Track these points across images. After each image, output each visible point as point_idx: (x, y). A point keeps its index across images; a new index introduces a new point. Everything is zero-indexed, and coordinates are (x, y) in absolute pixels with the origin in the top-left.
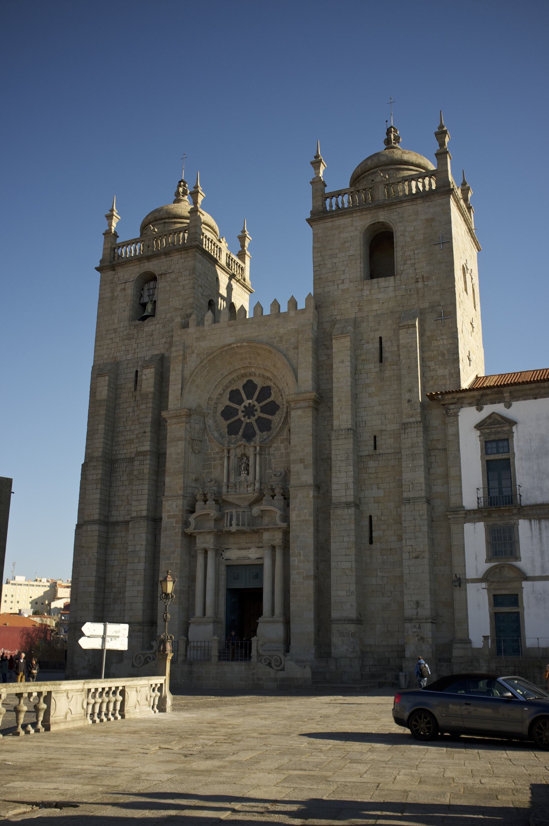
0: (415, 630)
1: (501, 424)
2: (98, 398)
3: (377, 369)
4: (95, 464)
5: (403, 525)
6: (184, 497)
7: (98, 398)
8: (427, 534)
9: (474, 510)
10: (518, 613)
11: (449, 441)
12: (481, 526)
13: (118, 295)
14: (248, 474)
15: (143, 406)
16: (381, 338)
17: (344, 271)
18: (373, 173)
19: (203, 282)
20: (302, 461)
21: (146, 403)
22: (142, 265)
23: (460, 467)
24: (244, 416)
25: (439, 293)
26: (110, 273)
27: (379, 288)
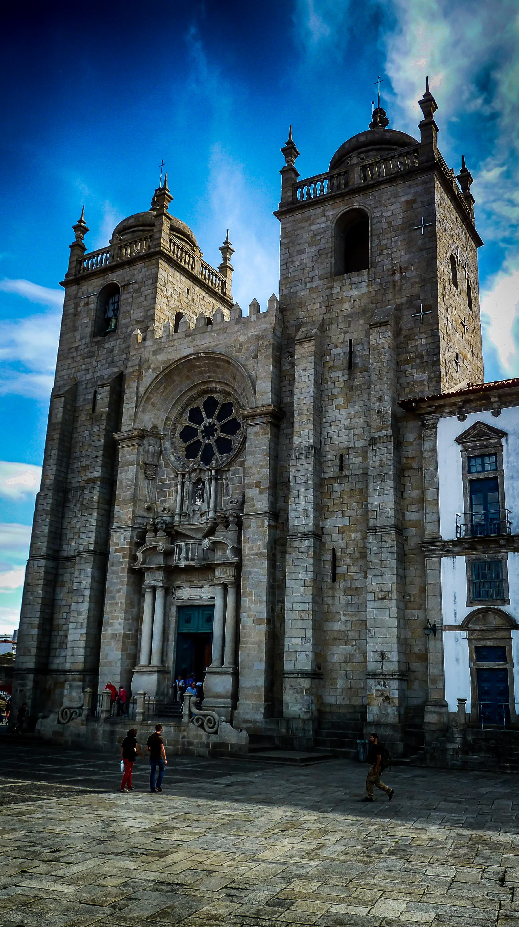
0: (379, 688)
1: (487, 436)
2: (54, 421)
3: (346, 377)
5: (369, 559)
6: (133, 528)
7: (54, 421)
8: (395, 570)
9: (453, 541)
10: (505, 670)
11: (425, 458)
12: (461, 561)
13: (81, 311)
14: (203, 501)
15: (96, 429)
17: (313, 267)
18: (350, 157)
19: (168, 292)
20: (257, 485)
21: (99, 425)
22: (106, 277)
23: (438, 489)
24: (203, 437)
25: (418, 285)
26: (74, 288)
27: (351, 284)
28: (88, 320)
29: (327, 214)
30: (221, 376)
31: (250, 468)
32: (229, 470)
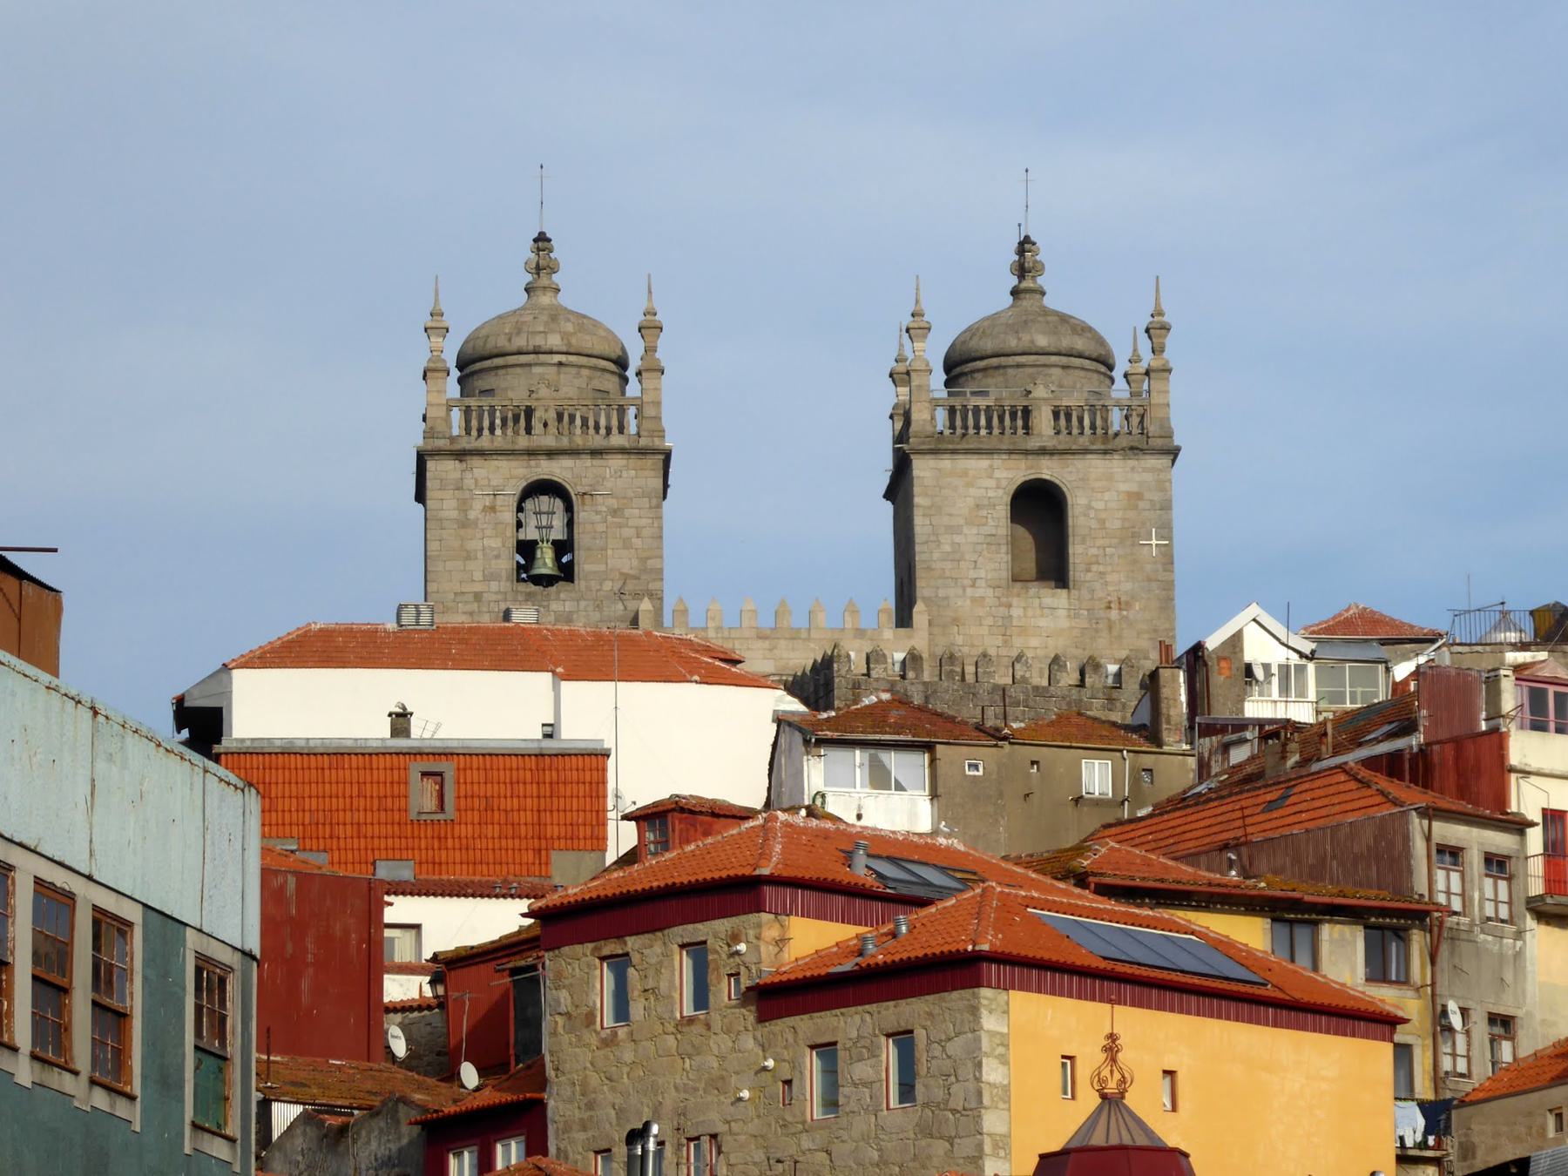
17: (975, 562)
18: (1018, 366)
22: (533, 463)
27: (1042, 608)
28: (500, 544)
29: (997, 474)
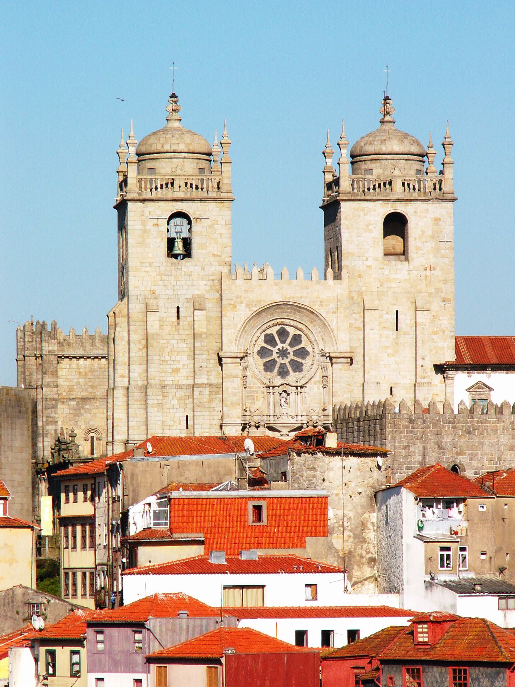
3: (395, 336)
4: (155, 390)
16: (397, 311)
18: (386, 159)
30: (298, 317)
31: (337, 392)
32: (306, 387)
